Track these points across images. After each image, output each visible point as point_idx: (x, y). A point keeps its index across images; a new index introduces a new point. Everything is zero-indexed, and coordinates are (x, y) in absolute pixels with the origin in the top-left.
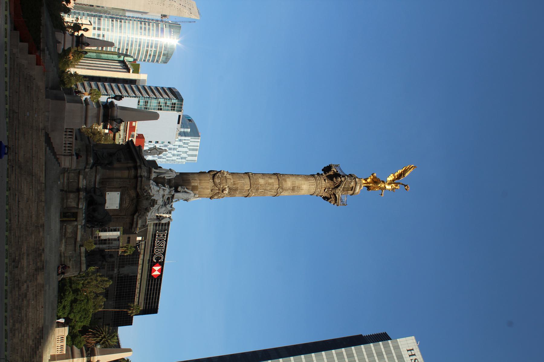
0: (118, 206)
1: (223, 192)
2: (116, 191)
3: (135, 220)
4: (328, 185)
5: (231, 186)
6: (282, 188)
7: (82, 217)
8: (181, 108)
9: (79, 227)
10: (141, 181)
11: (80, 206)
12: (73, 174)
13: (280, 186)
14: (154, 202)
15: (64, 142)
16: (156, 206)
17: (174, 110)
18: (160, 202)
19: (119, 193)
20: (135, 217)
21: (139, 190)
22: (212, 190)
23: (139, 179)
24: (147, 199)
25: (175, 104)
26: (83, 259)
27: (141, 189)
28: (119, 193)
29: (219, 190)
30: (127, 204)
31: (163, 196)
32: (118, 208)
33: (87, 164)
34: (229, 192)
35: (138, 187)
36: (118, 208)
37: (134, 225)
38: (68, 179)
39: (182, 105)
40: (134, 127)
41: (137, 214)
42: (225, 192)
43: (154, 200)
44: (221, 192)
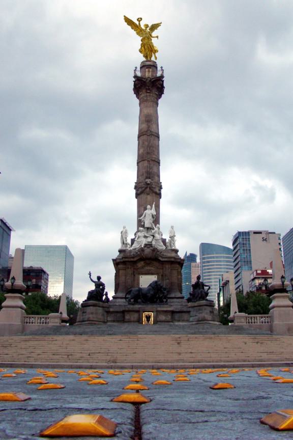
0: (154, 276)
1: (148, 184)
3: (166, 260)
4: (144, 91)
5: (145, 177)
6: (146, 131)
8: (245, 232)
9: (159, 309)
10: (125, 258)
12: (108, 318)
13: (144, 133)
14: (148, 245)
15: (39, 324)
16: (154, 243)
17: (249, 239)
18: (150, 239)
19: (140, 276)
20: (164, 260)
21: (135, 259)
22: (148, 194)
23: (124, 260)
25: (243, 238)
26: (196, 304)
27: (133, 258)
28: (140, 276)
29: (146, 188)
30: (152, 268)
31: (145, 237)
32: (156, 276)
33: (94, 305)
34: (150, 178)
35: (132, 260)
36: (156, 276)
37: (173, 260)
38: (114, 321)
39: (243, 232)
40: (262, 271)
41: (160, 258)
42: (149, 182)
43: (145, 244)
44: (149, 186)
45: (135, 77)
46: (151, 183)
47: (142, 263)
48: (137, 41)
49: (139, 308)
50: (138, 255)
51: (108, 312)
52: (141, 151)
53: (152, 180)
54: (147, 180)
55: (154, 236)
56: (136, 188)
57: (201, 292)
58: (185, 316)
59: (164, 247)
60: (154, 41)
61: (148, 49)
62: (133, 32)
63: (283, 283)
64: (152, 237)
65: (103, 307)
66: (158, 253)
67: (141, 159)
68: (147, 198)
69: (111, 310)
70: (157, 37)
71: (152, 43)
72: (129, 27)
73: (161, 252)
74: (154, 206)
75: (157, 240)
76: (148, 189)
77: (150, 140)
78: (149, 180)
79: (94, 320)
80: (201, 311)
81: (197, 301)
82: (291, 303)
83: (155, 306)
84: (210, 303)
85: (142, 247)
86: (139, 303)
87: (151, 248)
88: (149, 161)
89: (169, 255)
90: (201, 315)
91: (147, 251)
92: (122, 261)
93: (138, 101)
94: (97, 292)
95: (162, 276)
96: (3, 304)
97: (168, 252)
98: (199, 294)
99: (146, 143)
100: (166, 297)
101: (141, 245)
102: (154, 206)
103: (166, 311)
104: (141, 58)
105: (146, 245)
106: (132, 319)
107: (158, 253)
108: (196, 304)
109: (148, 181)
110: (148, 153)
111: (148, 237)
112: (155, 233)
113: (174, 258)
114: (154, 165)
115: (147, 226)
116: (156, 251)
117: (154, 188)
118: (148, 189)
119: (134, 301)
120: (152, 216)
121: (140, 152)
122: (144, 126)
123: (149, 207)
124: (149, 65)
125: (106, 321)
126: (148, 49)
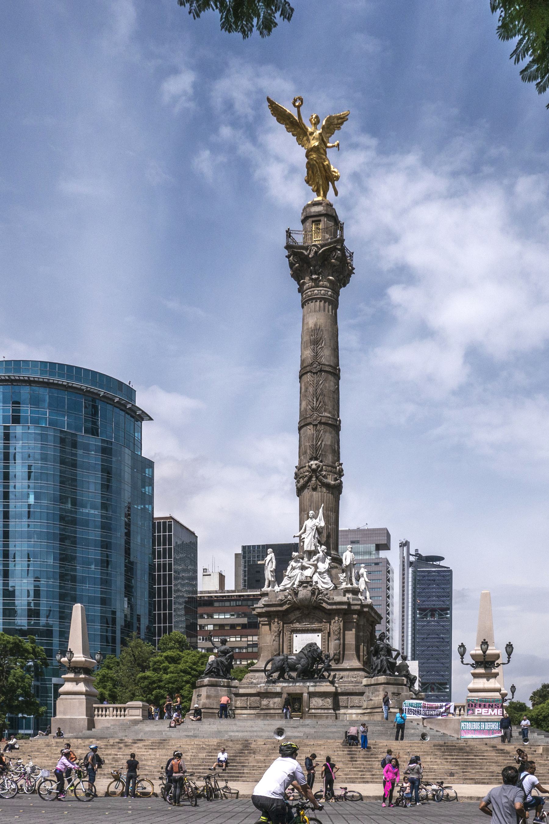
2: (291, 641)
3: (334, 607)
5: (308, 458)
6: (312, 364)
7: (298, 687)
9: (312, 689)
11: (278, 690)
12: (238, 702)
13: (308, 369)
14: (306, 583)
16: (316, 578)
18: (308, 572)
19: (295, 635)
20: (329, 607)
21: (285, 607)
24: (296, 594)
26: (373, 681)
27: (281, 605)
32: (320, 635)
34: (316, 459)
37: (345, 607)
38: (245, 708)
41: (324, 605)
42: (314, 467)
46: (318, 467)
47: (298, 614)
49: (283, 688)
50: (289, 600)
51: (237, 695)
52: (304, 403)
53: (321, 462)
54: (312, 462)
55: (316, 567)
57: (382, 661)
58: (356, 700)
59: (331, 585)
64: (313, 568)
65: (229, 686)
66: (320, 597)
68: (312, 496)
69: (241, 691)
73: (327, 594)
74: (321, 510)
75: (320, 573)
76: (314, 479)
77: (318, 383)
78: (316, 462)
79: (212, 707)
80: (377, 693)
81: (374, 676)
83: (308, 684)
84: (395, 680)
85: (295, 586)
86: (286, 681)
87: (310, 588)
88: (316, 425)
89: (338, 599)
90: (377, 698)
91: (303, 593)
92: (264, 610)
94: (218, 664)
95: (329, 634)
97: (338, 595)
98: (377, 666)
99: (311, 389)
100: (328, 669)
101: (294, 584)
102: (321, 510)
105: (301, 583)
106: (272, 706)
107: (320, 597)
108: (373, 681)
109: (313, 463)
110: (314, 409)
111: (307, 568)
112: (318, 560)
113: (349, 604)
114: (325, 432)
115: (309, 549)
116: (317, 592)
117: (325, 477)
118: (314, 479)
119: (279, 677)
120: (317, 529)
123: (311, 513)
125: (234, 708)
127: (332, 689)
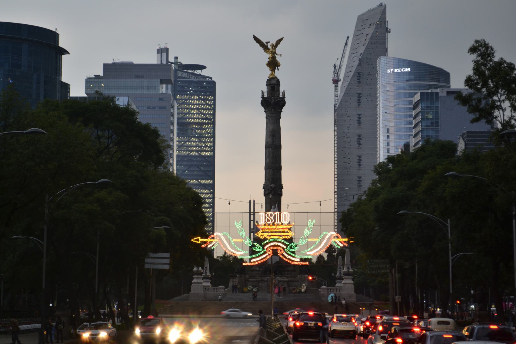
11: (266, 280)
45: (263, 97)
48: (266, 57)
56: (264, 188)
60: (278, 58)
61: (273, 64)
62: (261, 49)
63: (348, 271)
67: (267, 168)
69: (250, 280)
70: (281, 55)
71: (277, 61)
72: (258, 45)
82: (353, 282)
93: (264, 115)
96: (193, 281)
103: (284, 281)
104: (267, 72)
121: (267, 161)
122: (270, 140)
124: (273, 84)
126: (273, 64)
127: (287, 280)
